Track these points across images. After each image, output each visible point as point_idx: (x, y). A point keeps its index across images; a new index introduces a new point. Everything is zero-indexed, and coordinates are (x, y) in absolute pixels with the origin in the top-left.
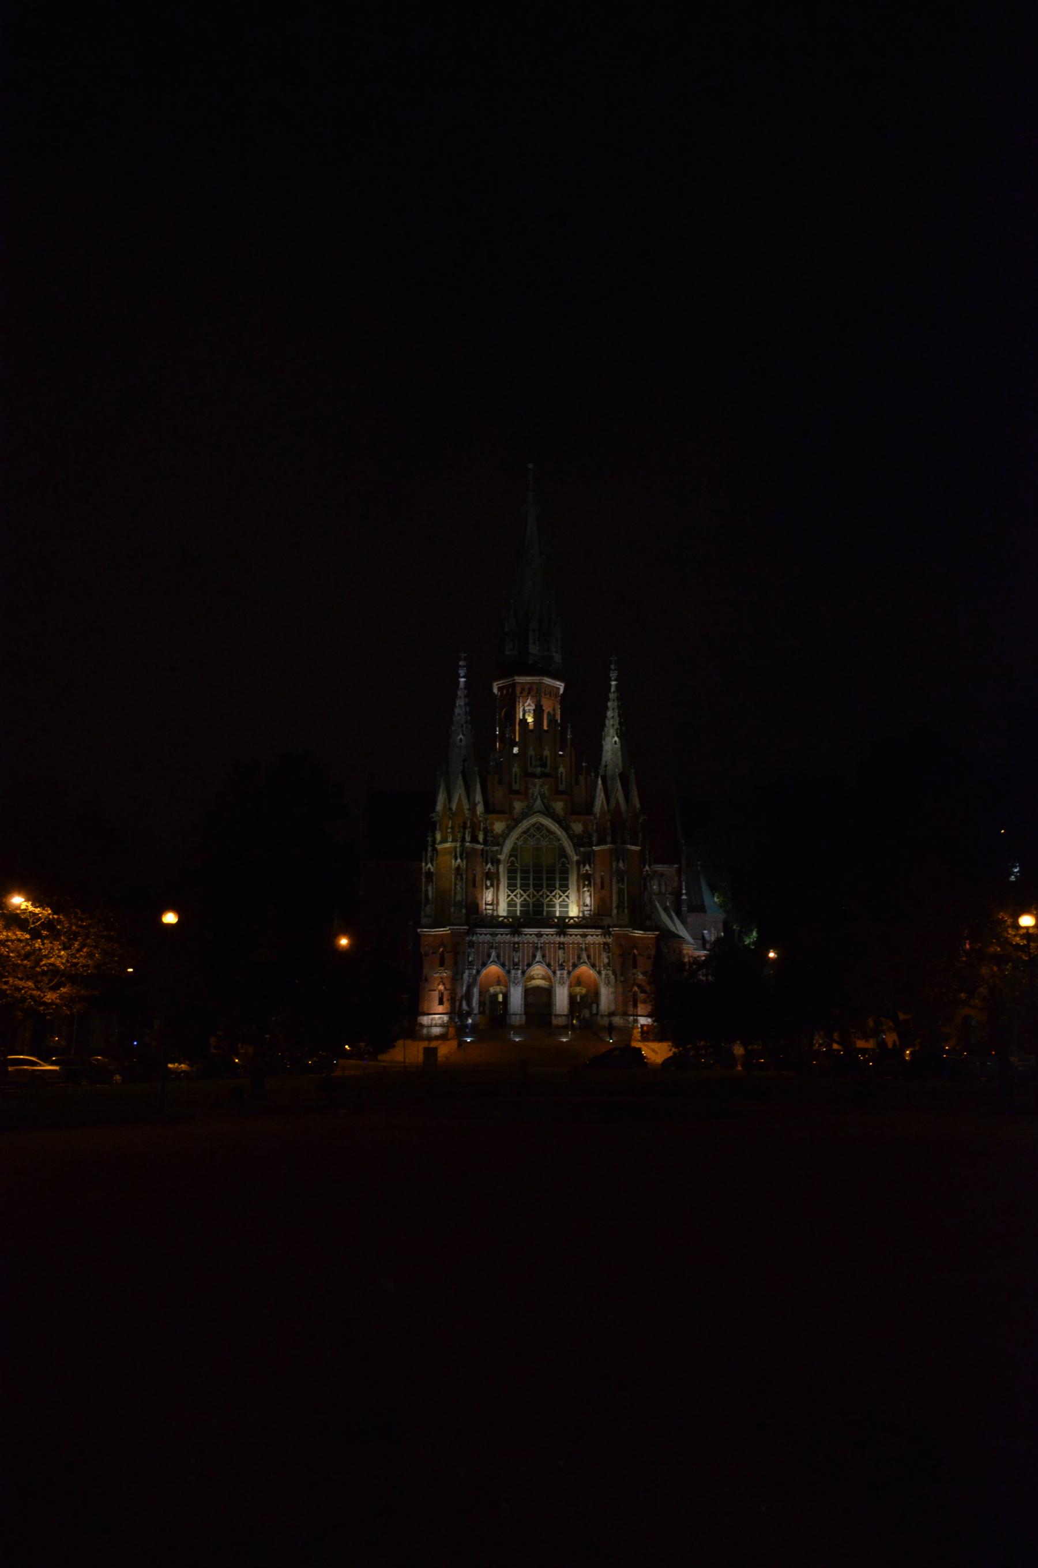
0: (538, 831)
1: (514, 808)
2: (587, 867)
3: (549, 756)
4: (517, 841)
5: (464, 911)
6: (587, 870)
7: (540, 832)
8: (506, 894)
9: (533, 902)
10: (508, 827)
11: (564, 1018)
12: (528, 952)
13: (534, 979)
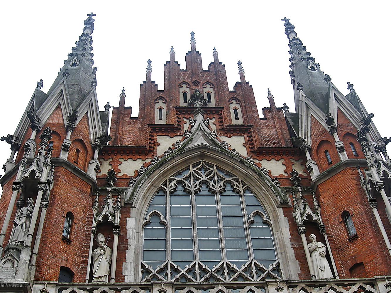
2: (309, 211)
6: (309, 216)
7: (207, 176)
8: (140, 269)
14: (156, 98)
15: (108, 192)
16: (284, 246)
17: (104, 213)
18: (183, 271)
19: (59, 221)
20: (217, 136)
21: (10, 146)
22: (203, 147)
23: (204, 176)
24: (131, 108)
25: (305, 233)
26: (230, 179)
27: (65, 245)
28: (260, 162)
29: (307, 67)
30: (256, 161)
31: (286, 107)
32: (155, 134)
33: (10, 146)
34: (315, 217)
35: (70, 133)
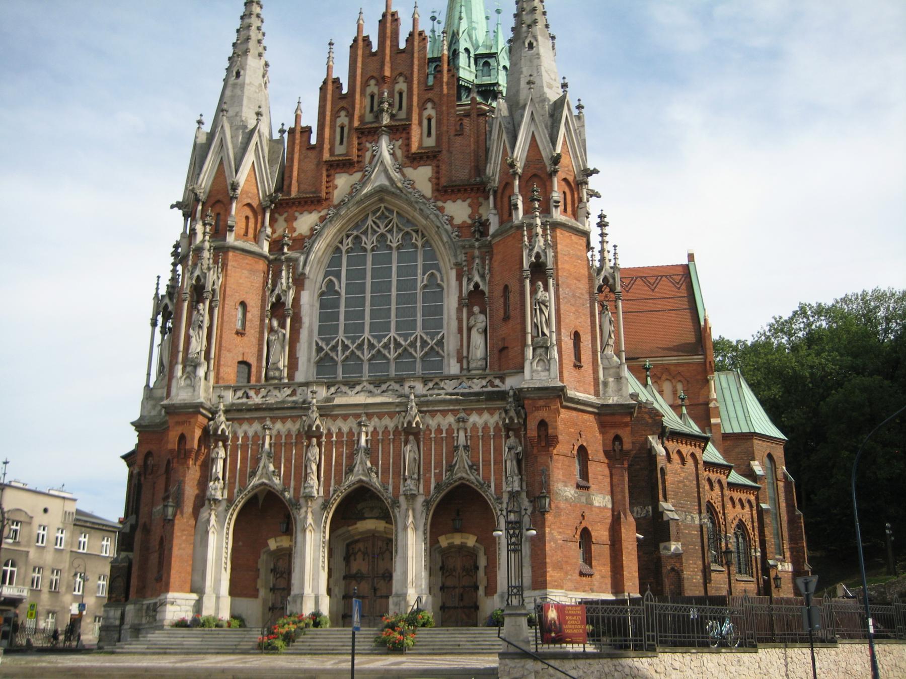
0: (383, 223)
2: (477, 278)
4: (340, 245)
6: (477, 286)
8: (314, 347)
9: (370, 360)
10: (322, 219)
13: (363, 518)
14: (337, 109)
15: (282, 262)
16: (449, 318)
17: (276, 292)
18: (353, 347)
19: (232, 315)
20: (400, 169)
21: (181, 212)
22: (381, 190)
23: (382, 227)
24: (307, 131)
25: (467, 306)
26: (409, 229)
27: (239, 338)
28: (443, 204)
29: (524, 43)
30: (440, 204)
32: (332, 172)
33: (181, 212)
34: (481, 287)
35: (234, 205)
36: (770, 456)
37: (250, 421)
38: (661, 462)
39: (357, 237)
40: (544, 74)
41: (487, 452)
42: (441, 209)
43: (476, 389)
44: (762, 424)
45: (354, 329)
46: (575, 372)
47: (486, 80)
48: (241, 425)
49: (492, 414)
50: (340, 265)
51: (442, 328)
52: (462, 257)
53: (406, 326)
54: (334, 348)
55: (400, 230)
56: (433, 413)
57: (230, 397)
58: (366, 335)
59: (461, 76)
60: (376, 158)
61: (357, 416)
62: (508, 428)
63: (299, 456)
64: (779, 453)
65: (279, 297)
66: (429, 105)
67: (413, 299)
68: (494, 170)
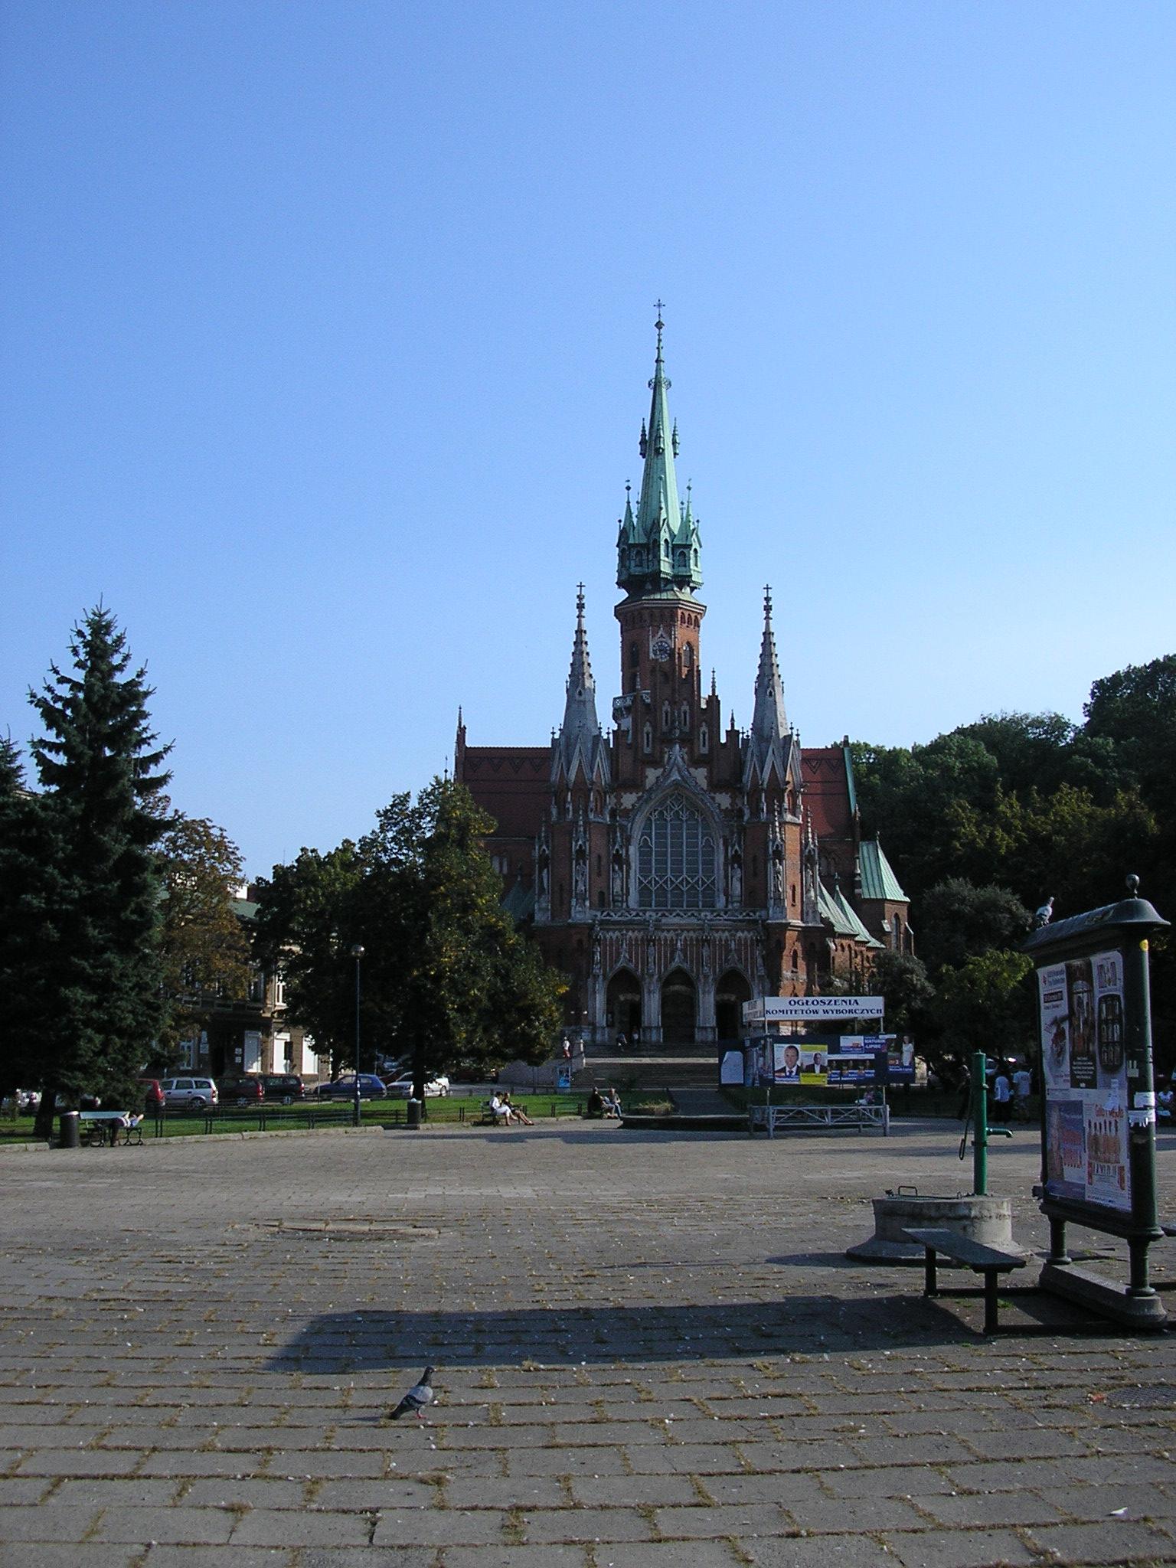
1: (647, 777)
2: (737, 847)
3: (688, 711)
5: (587, 903)
6: (736, 851)
10: (639, 798)
11: (709, 1030)
12: (665, 953)
22: (676, 784)
30: (712, 795)
31: (743, 733)
36: (896, 916)
37: (614, 931)
38: (832, 954)
39: (661, 813)
40: (779, 716)
41: (746, 953)
42: (713, 798)
43: (740, 917)
44: (893, 890)
45: (661, 871)
46: (792, 909)
47: (682, 571)
48: (608, 932)
49: (749, 932)
50: (651, 829)
51: (713, 872)
52: (727, 832)
53: (693, 872)
54: (650, 882)
55: (687, 809)
56: (717, 931)
57: (599, 917)
58: (669, 875)
59: (662, 569)
60: (672, 761)
61: (675, 930)
62: (757, 940)
63: (643, 952)
64: (904, 913)
65: (617, 851)
66: (704, 724)
67: (704, 863)
68: (747, 777)
